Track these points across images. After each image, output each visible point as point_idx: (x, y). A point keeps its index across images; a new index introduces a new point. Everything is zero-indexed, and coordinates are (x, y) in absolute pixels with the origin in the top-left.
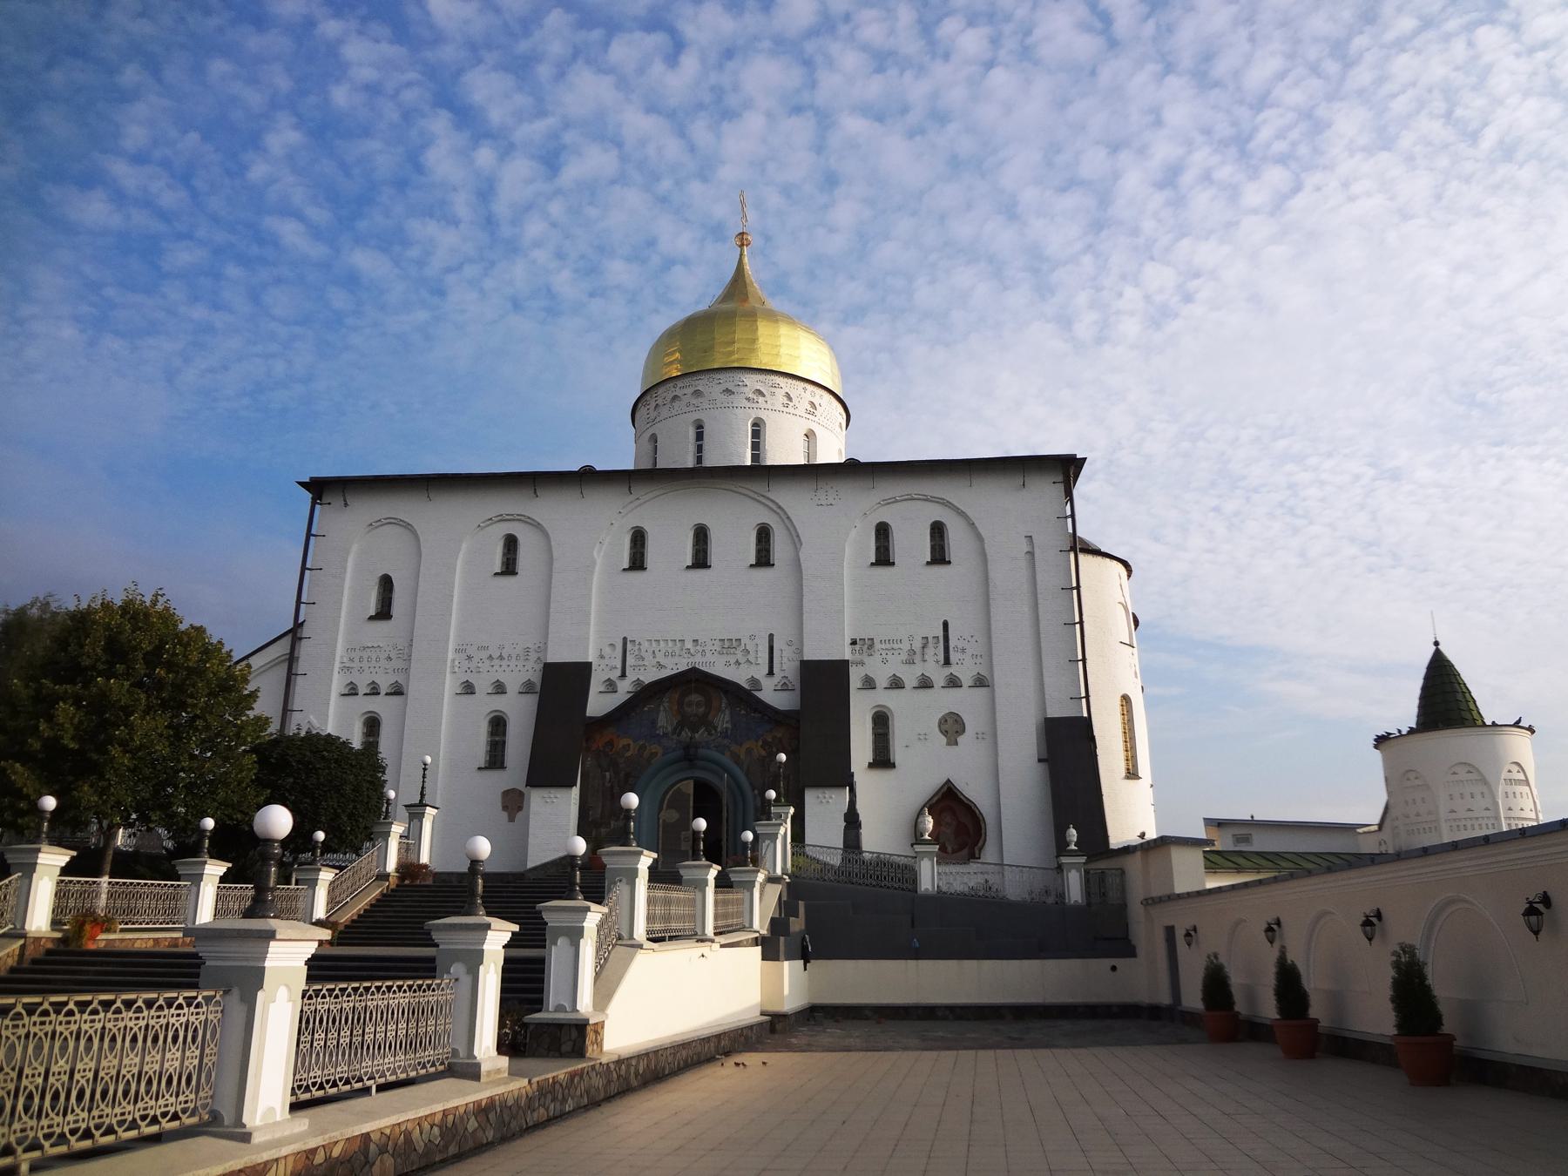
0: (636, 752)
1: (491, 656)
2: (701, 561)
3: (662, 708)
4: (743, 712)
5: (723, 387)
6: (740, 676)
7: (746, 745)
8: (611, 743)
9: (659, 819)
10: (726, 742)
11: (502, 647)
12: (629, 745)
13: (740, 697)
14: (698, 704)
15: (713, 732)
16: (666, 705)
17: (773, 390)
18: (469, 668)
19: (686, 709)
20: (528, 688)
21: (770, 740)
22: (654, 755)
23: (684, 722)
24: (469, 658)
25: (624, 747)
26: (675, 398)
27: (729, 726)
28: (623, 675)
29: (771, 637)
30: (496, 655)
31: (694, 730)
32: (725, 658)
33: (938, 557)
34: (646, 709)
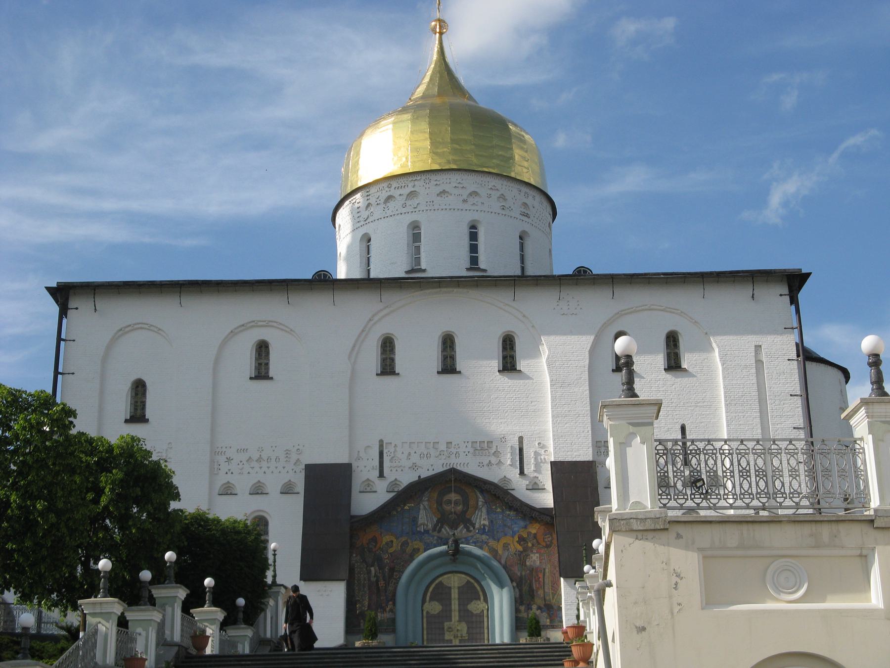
0: (399, 548)
1: (250, 457)
3: (422, 507)
4: (499, 510)
5: (440, 189)
7: (504, 540)
8: (374, 540)
9: (422, 611)
10: (484, 537)
11: (261, 450)
12: (392, 542)
14: (456, 503)
15: (472, 529)
16: (426, 503)
17: (490, 192)
18: (229, 470)
19: (445, 506)
20: (287, 490)
21: (525, 536)
22: (416, 552)
23: (444, 520)
24: (229, 460)
25: (387, 544)
26: (389, 198)
27: (486, 523)
28: (381, 475)
29: (521, 439)
30: (256, 456)
31: (454, 526)
33: (673, 364)
34: (406, 507)
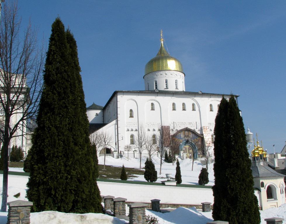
2: (184, 109)
6: (192, 128)
13: (193, 132)
14: (187, 133)
23: (185, 136)
24: (148, 125)
28: (174, 128)
29: (196, 122)
32: (190, 126)
